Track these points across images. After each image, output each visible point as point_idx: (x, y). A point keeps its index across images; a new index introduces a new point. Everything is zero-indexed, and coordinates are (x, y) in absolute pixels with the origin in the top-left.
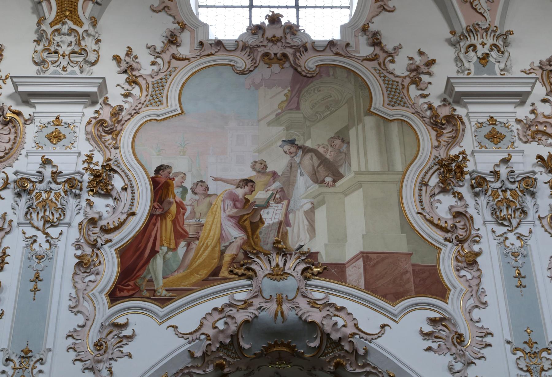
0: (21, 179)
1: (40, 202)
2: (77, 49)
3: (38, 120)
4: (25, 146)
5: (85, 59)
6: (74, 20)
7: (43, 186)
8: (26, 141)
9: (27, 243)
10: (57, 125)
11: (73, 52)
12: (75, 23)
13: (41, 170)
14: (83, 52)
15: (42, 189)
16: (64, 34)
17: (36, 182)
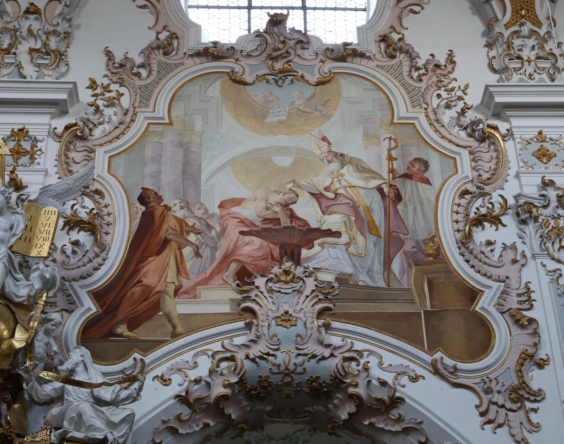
0: (525, 203)
1: (550, 230)
2: (541, 54)
3: (519, 136)
4: (511, 165)
5: (554, 65)
6: (532, 21)
7: (548, 212)
8: (510, 159)
9: (551, 277)
10: (542, 141)
11: (539, 58)
12: (533, 24)
13: (543, 192)
14: (550, 58)
15: (548, 215)
16: (524, 37)
17: (539, 207)
